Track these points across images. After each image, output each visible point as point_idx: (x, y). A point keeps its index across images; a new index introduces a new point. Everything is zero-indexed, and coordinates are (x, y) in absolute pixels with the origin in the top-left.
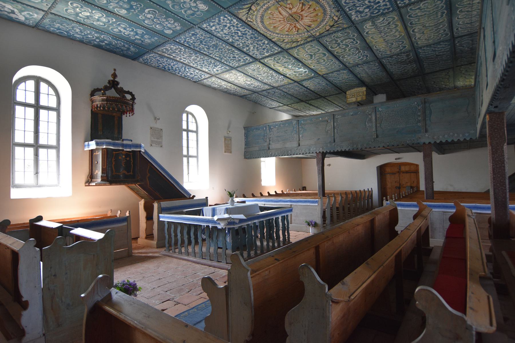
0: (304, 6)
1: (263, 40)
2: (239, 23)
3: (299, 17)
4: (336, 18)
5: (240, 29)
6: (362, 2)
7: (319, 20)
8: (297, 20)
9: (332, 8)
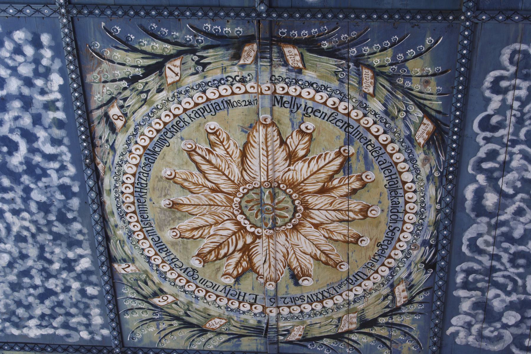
0: (341, 175)
1: (79, 244)
2: (59, 104)
3: (296, 211)
4: (405, 294)
5: (41, 134)
6: (521, 270)
7: (345, 268)
8: (279, 221)
9: (419, 243)
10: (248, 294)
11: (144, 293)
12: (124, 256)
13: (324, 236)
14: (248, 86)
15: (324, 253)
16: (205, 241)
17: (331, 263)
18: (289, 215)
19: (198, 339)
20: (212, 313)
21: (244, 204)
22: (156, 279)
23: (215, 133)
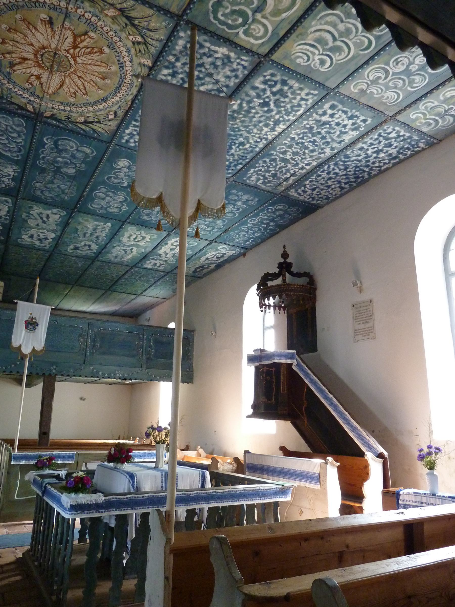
0: (15, 62)
3: (42, 56)
7: (18, 16)
8: (52, 54)
10: (84, 22)
11: (144, 46)
12: (143, 67)
13: (28, 38)
14: (51, 106)
15: (29, 29)
16: (96, 58)
17: (27, 23)
18: (46, 55)
19: (128, 7)
20: (111, 20)
21: (68, 68)
22: (133, 51)
23: (72, 97)
